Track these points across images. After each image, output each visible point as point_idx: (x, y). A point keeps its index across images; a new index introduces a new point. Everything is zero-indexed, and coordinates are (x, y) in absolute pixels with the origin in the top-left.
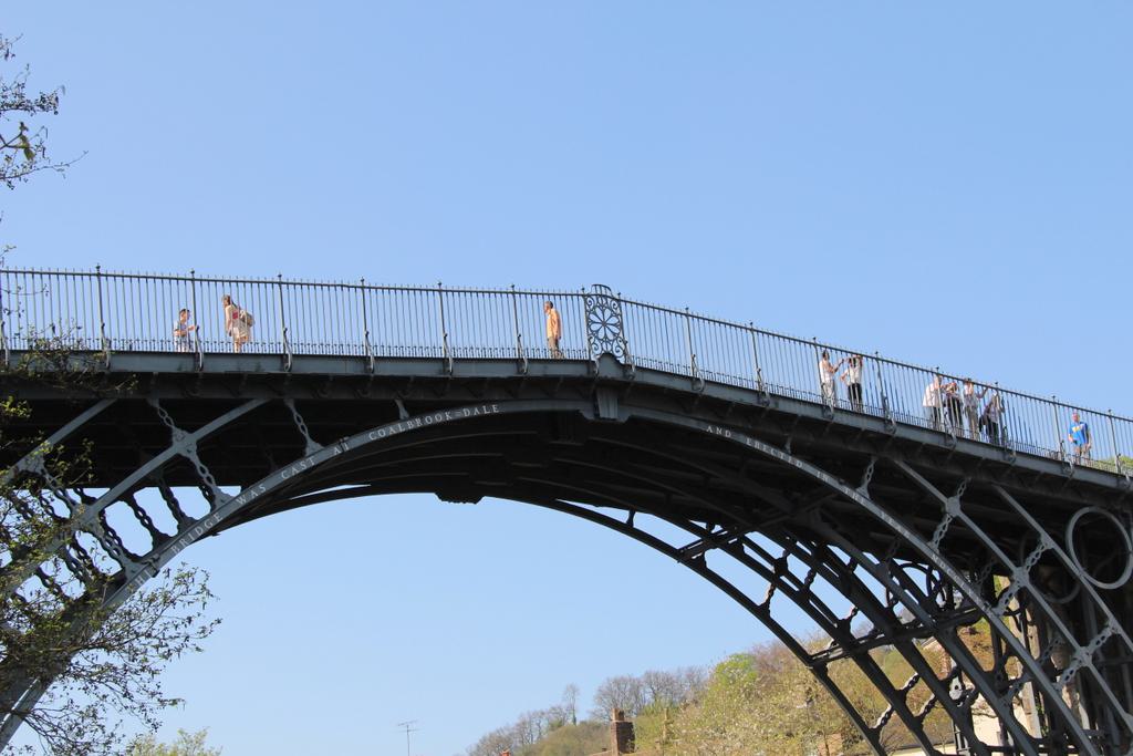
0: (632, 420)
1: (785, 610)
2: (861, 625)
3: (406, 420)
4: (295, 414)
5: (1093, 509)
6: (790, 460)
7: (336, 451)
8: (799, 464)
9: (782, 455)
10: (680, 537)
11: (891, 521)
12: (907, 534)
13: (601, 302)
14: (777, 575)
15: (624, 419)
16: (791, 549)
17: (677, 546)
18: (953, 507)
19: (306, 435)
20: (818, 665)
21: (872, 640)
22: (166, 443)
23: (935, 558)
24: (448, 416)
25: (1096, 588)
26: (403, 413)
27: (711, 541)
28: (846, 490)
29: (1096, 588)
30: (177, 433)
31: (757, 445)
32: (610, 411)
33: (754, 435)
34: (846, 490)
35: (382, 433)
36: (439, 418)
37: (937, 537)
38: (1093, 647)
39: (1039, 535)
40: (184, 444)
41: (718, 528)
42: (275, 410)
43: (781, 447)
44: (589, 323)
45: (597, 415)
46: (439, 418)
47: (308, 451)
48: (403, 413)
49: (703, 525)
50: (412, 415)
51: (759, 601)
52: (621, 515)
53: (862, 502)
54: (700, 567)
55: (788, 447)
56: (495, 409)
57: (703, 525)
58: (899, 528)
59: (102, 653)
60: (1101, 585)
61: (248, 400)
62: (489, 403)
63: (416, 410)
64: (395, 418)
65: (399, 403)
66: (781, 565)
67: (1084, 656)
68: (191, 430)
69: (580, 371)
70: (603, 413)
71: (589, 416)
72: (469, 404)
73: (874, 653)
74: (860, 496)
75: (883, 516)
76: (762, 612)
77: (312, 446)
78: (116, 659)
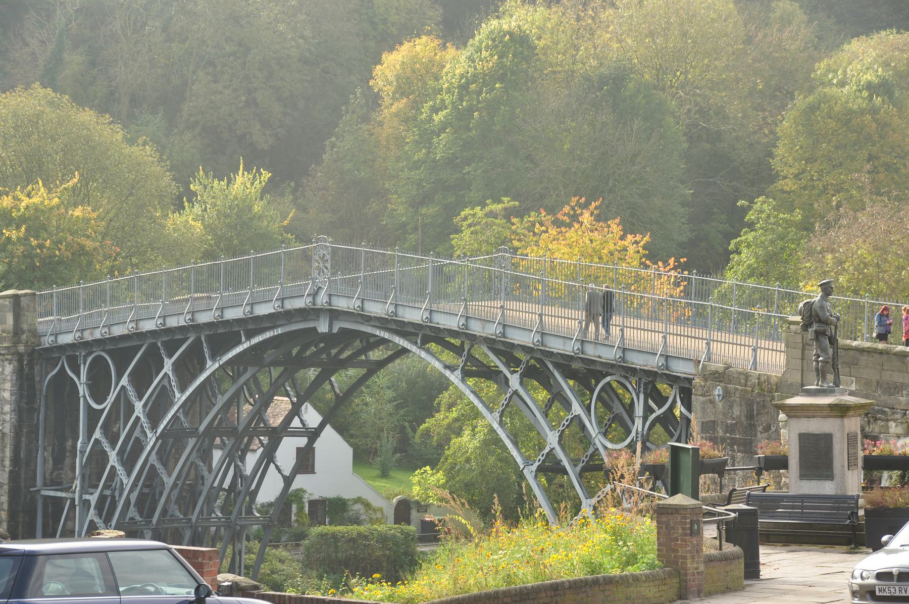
3: (245, 342)
15: (335, 330)
24: (261, 339)
30: (166, 360)
32: (323, 327)
42: (198, 341)
43: (416, 343)
47: (207, 366)
48: (243, 339)
55: (419, 342)
56: (280, 331)
61: (189, 338)
63: (250, 335)
64: (239, 342)
65: (242, 332)
71: (319, 331)
77: (209, 363)
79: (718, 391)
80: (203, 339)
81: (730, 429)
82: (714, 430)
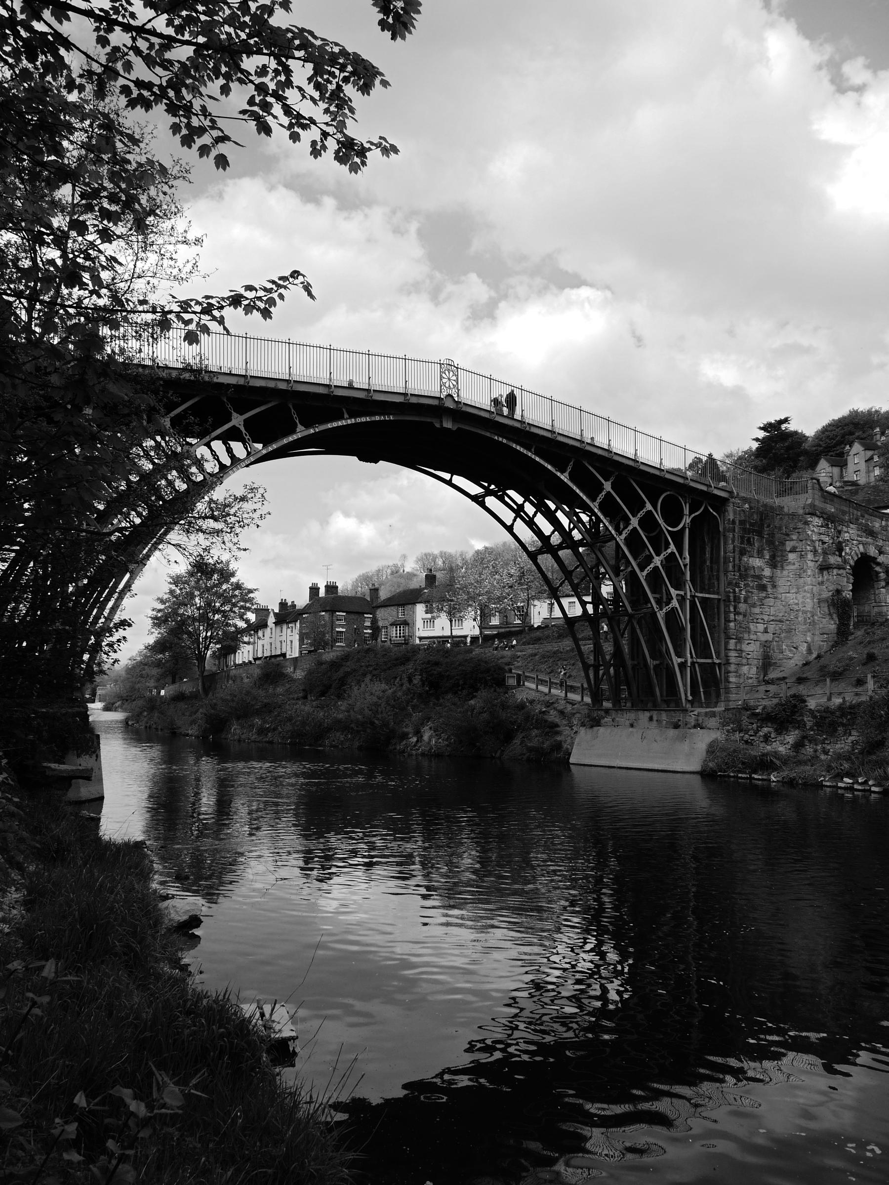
0: (459, 428)
1: (521, 528)
2: (556, 539)
3: (347, 419)
4: (293, 410)
5: (671, 493)
6: (533, 457)
7: (312, 431)
8: (537, 459)
9: (530, 454)
10: (475, 490)
11: (578, 491)
12: (584, 498)
13: (449, 367)
14: (519, 511)
15: (455, 429)
16: (527, 499)
17: (473, 493)
18: (608, 486)
19: (298, 422)
20: (533, 556)
21: (560, 547)
22: (230, 420)
23: (596, 510)
24: (368, 419)
25: (667, 529)
26: (346, 416)
27: (489, 492)
28: (559, 474)
29: (667, 529)
30: (235, 415)
31: (518, 448)
32: (448, 424)
33: (518, 443)
34: (559, 474)
35: (335, 424)
36: (363, 419)
37: (598, 500)
38: (662, 557)
39: (645, 503)
40: (237, 420)
41: (493, 487)
43: (530, 451)
44: (441, 377)
45: (442, 425)
46: (363, 419)
47: (298, 430)
48: (346, 416)
49: (486, 484)
50: (350, 418)
51: (509, 523)
52: (447, 476)
53: (566, 480)
54: (482, 505)
55: (533, 450)
57: (486, 484)
58: (581, 494)
59: (211, 521)
60: (670, 529)
61: (271, 401)
62: (389, 414)
64: (341, 418)
65: (344, 410)
66: (521, 507)
67: (657, 561)
68: (241, 414)
69: (436, 402)
70: (445, 425)
71: (438, 425)
72: (380, 414)
73: (560, 553)
74: (564, 477)
75: (575, 488)
76: (510, 529)
77: (300, 427)
78: (218, 526)
79: (747, 506)
80: (291, 407)
81: (751, 524)
82: (745, 524)
